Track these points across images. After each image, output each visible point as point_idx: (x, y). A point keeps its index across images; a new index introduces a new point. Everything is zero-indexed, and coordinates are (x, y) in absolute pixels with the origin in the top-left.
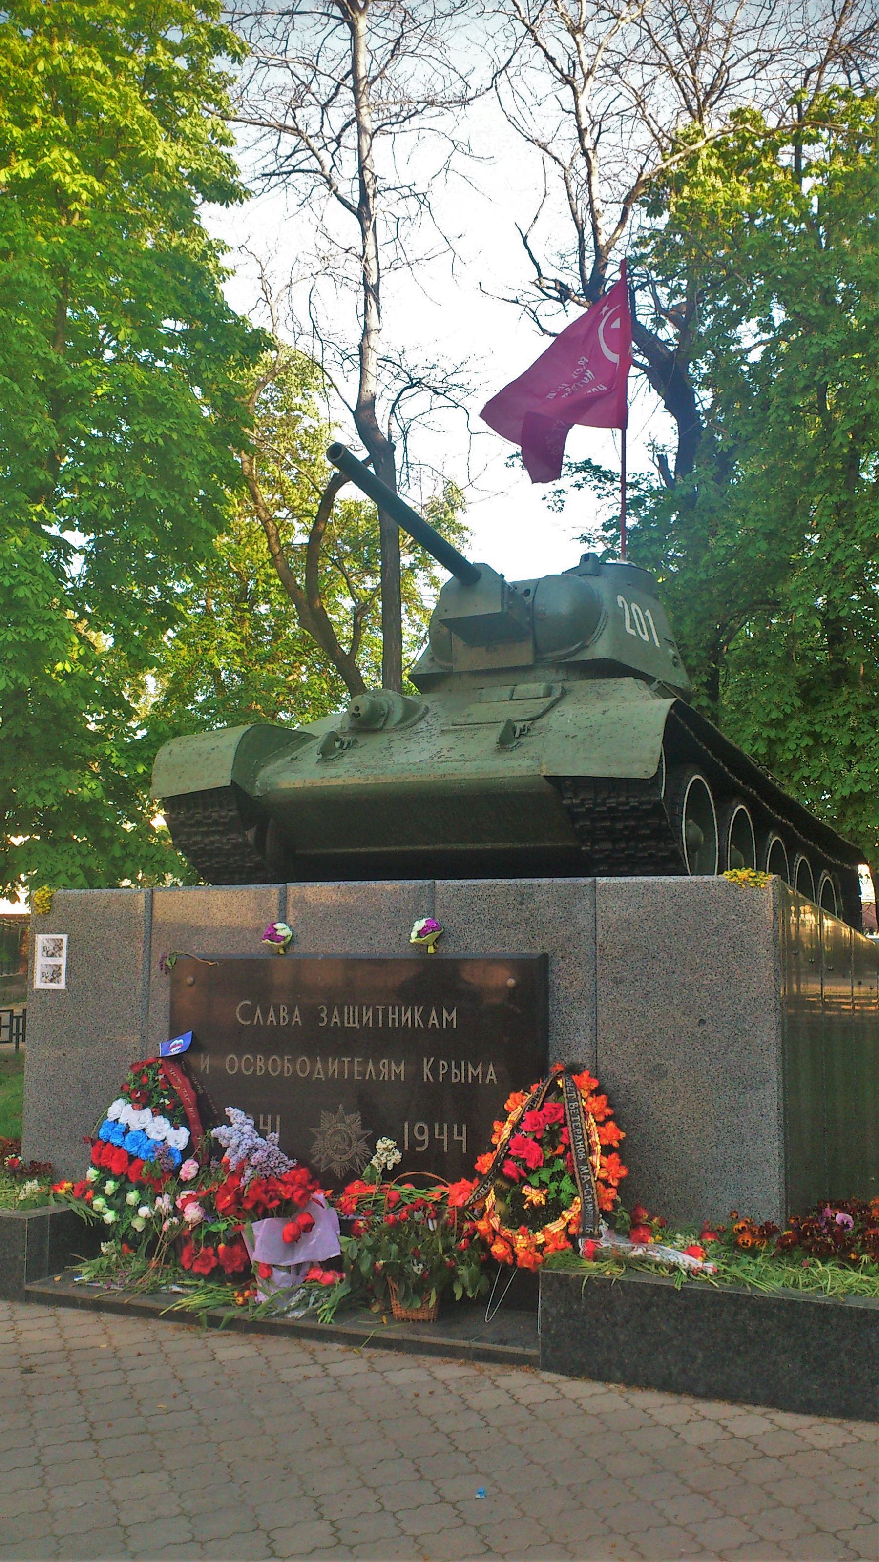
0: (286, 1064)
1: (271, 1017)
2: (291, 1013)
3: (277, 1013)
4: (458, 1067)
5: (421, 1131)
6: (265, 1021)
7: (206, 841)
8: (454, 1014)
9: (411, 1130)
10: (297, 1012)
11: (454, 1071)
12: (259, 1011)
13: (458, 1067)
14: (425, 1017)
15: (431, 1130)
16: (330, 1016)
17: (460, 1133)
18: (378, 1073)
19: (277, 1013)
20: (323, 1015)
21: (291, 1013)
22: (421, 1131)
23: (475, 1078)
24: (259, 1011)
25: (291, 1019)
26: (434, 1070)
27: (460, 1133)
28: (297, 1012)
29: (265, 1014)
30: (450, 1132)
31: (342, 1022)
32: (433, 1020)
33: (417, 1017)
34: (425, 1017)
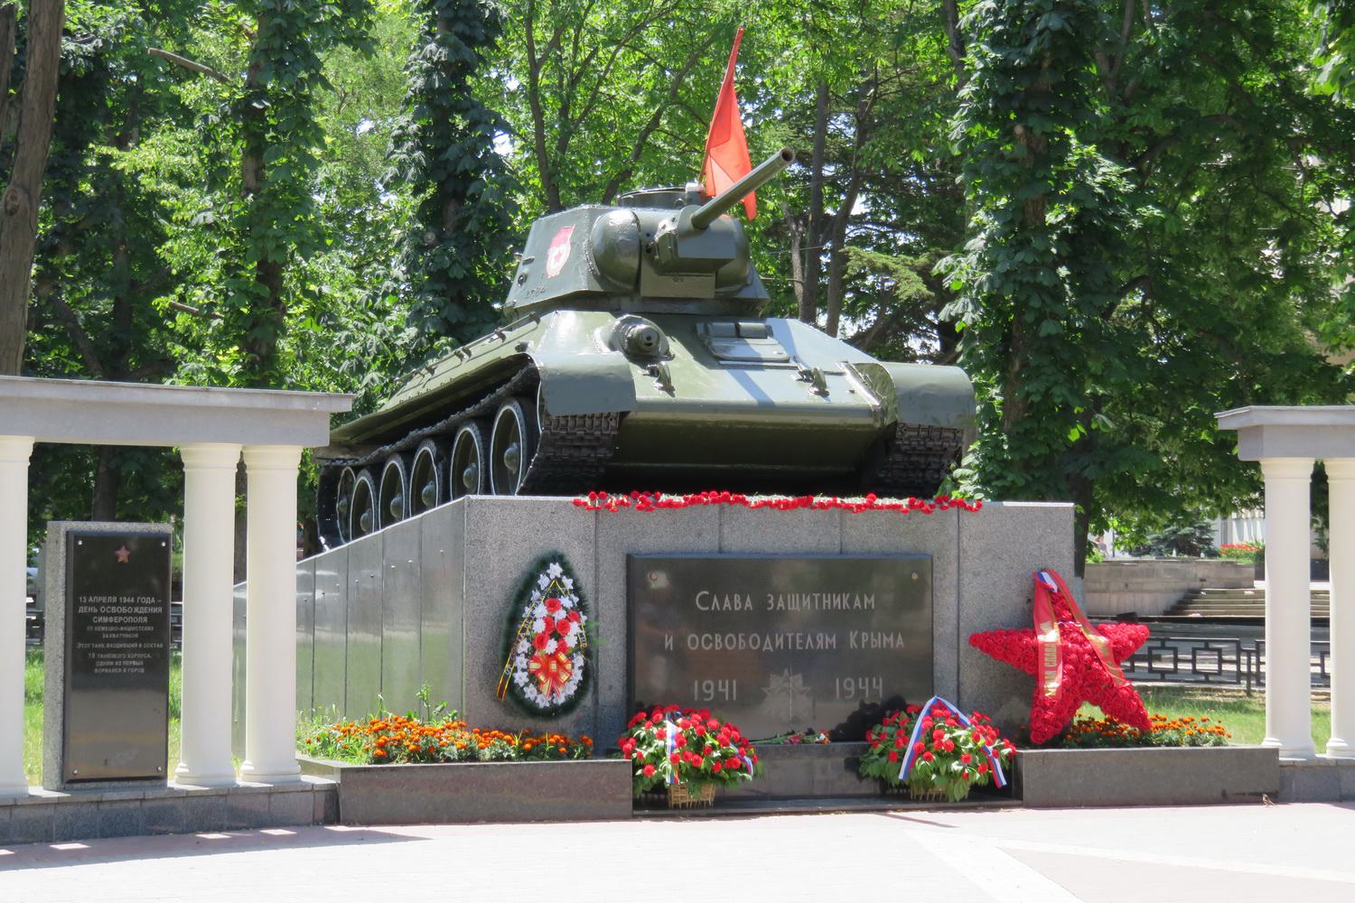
0: (741, 640)
1: (727, 604)
2: (743, 601)
3: (732, 600)
4: (876, 637)
5: (849, 684)
6: (721, 606)
7: (576, 453)
8: (873, 599)
9: (841, 685)
10: (748, 599)
11: (873, 639)
12: (715, 599)
13: (876, 637)
14: (851, 602)
15: (857, 682)
16: (776, 602)
17: (878, 683)
18: (815, 642)
19: (732, 600)
20: (771, 601)
21: (743, 601)
22: (849, 684)
23: (888, 644)
24: (715, 599)
25: (743, 605)
26: (858, 640)
27: (878, 683)
28: (748, 599)
29: (721, 602)
30: (857, 682)
31: (786, 605)
32: (857, 603)
33: (845, 602)
34: (851, 602)
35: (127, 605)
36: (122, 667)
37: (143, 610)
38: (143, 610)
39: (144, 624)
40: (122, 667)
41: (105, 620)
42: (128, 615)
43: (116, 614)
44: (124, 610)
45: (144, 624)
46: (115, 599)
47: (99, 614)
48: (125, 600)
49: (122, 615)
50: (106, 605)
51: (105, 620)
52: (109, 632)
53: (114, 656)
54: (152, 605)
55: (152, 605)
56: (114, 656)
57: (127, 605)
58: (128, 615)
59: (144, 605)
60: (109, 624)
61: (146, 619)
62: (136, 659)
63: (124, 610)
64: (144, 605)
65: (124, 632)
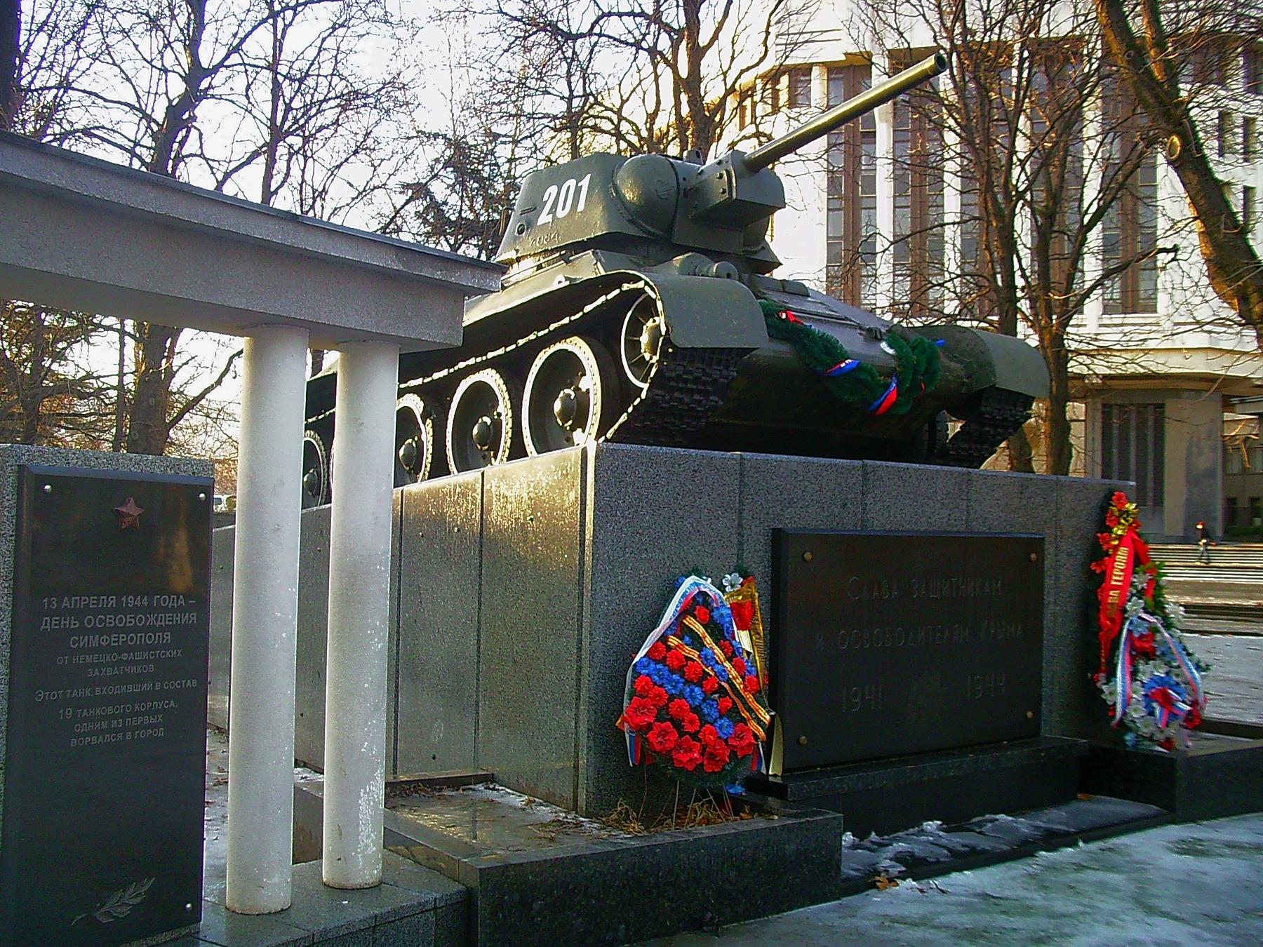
35: (135, 610)
36: (124, 730)
37: (165, 619)
38: (165, 619)
39: (167, 647)
40: (124, 730)
41: (94, 641)
42: (136, 629)
43: (115, 630)
44: (129, 621)
45: (167, 647)
46: (113, 602)
47: (82, 631)
48: (131, 601)
49: (126, 630)
50: (95, 612)
51: (94, 641)
52: (99, 665)
53: (110, 710)
54: (180, 609)
55: (180, 609)
56: (110, 710)
57: (135, 610)
58: (136, 629)
59: (166, 610)
60: (100, 650)
61: (168, 637)
62: (151, 712)
63: (129, 621)
64: (166, 610)
65: (129, 663)
